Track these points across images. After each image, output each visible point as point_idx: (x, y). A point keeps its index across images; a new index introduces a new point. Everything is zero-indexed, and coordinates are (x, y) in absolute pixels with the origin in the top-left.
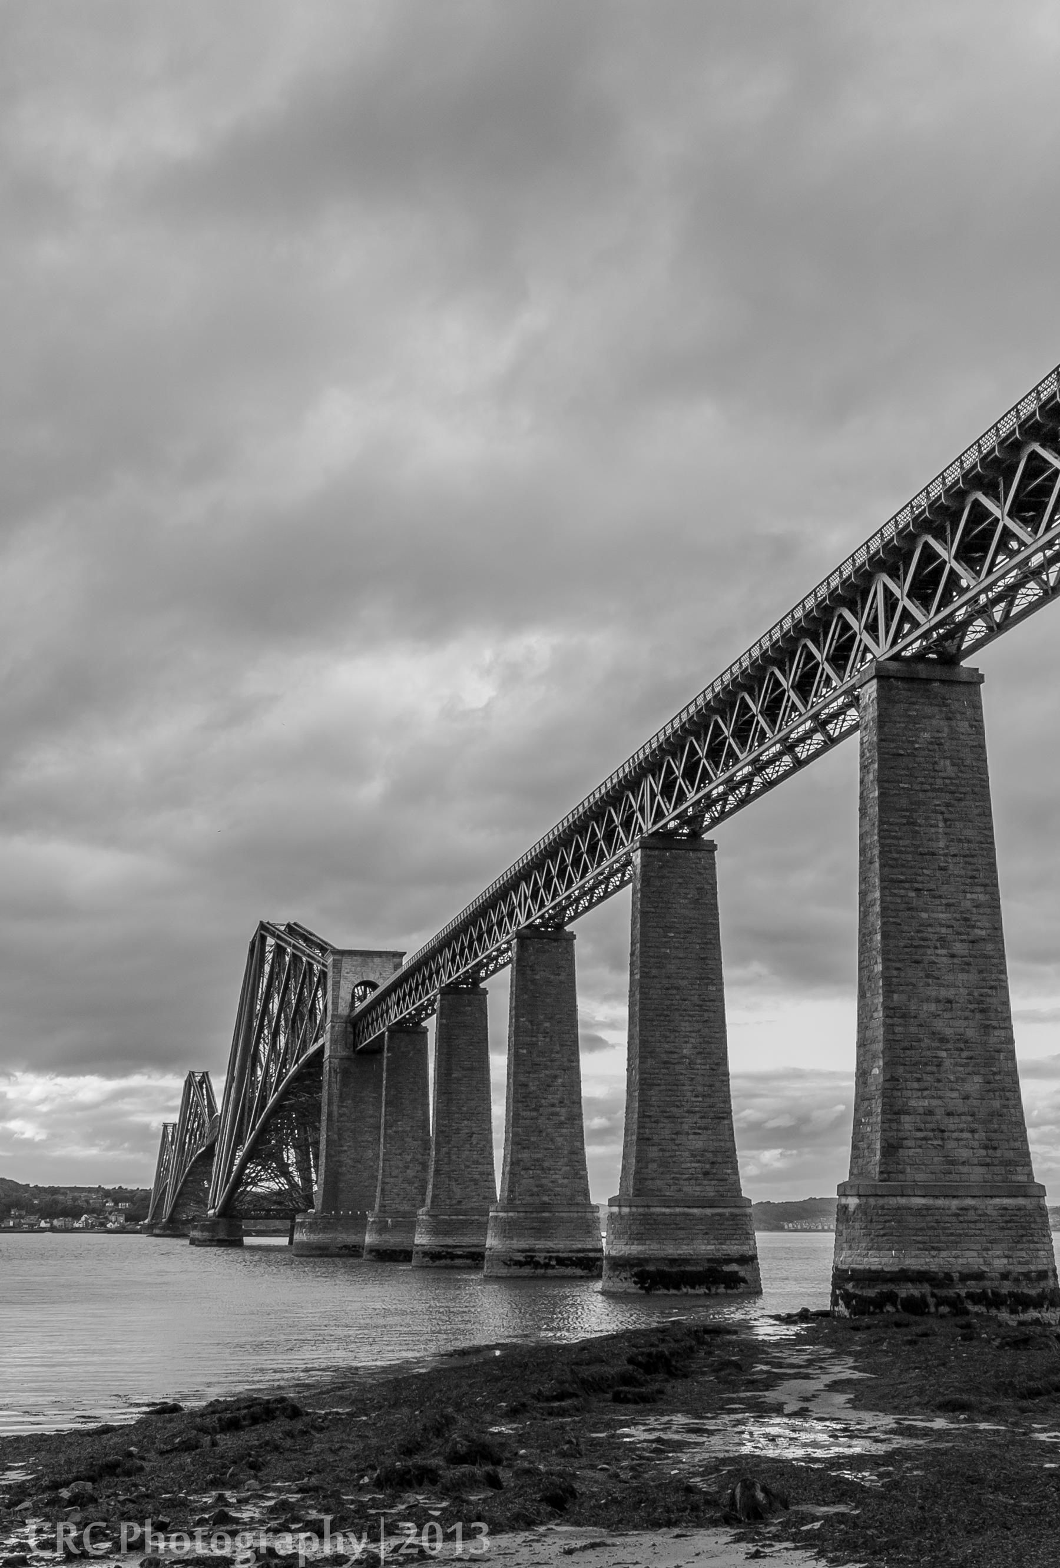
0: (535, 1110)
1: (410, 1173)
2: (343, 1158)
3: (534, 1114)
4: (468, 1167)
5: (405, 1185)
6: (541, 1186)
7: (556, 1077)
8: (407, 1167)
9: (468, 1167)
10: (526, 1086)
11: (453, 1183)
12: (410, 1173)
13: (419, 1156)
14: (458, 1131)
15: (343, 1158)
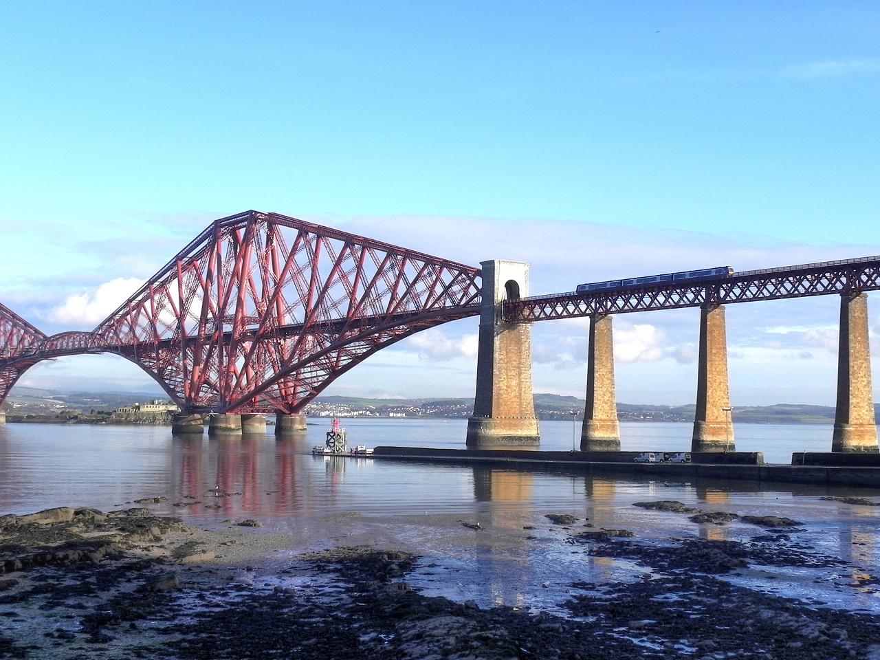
0: (857, 379)
1: (606, 398)
2: (501, 385)
3: (856, 381)
4: (719, 400)
5: (604, 404)
6: (859, 415)
7: (863, 363)
8: (604, 395)
9: (719, 400)
10: (853, 367)
11: (714, 408)
12: (606, 398)
13: (609, 389)
14: (715, 381)
15: (501, 385)
